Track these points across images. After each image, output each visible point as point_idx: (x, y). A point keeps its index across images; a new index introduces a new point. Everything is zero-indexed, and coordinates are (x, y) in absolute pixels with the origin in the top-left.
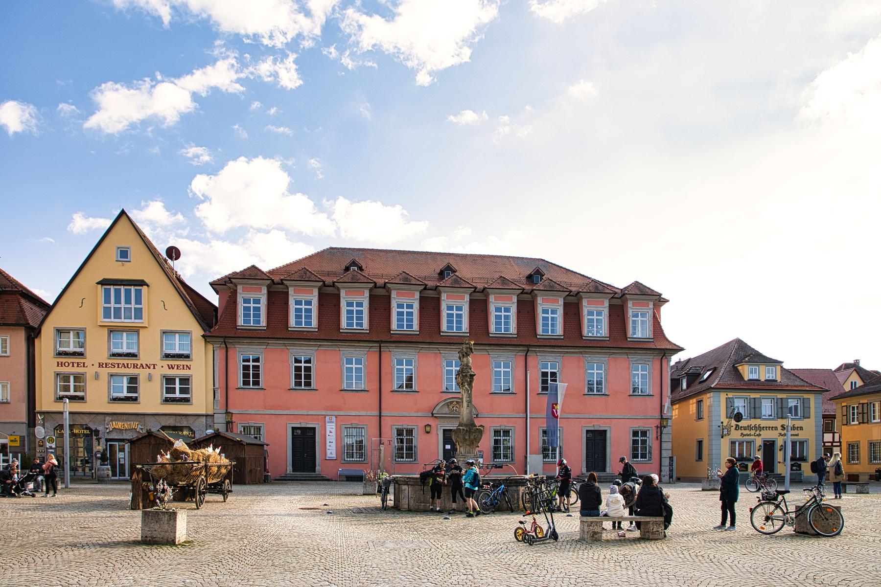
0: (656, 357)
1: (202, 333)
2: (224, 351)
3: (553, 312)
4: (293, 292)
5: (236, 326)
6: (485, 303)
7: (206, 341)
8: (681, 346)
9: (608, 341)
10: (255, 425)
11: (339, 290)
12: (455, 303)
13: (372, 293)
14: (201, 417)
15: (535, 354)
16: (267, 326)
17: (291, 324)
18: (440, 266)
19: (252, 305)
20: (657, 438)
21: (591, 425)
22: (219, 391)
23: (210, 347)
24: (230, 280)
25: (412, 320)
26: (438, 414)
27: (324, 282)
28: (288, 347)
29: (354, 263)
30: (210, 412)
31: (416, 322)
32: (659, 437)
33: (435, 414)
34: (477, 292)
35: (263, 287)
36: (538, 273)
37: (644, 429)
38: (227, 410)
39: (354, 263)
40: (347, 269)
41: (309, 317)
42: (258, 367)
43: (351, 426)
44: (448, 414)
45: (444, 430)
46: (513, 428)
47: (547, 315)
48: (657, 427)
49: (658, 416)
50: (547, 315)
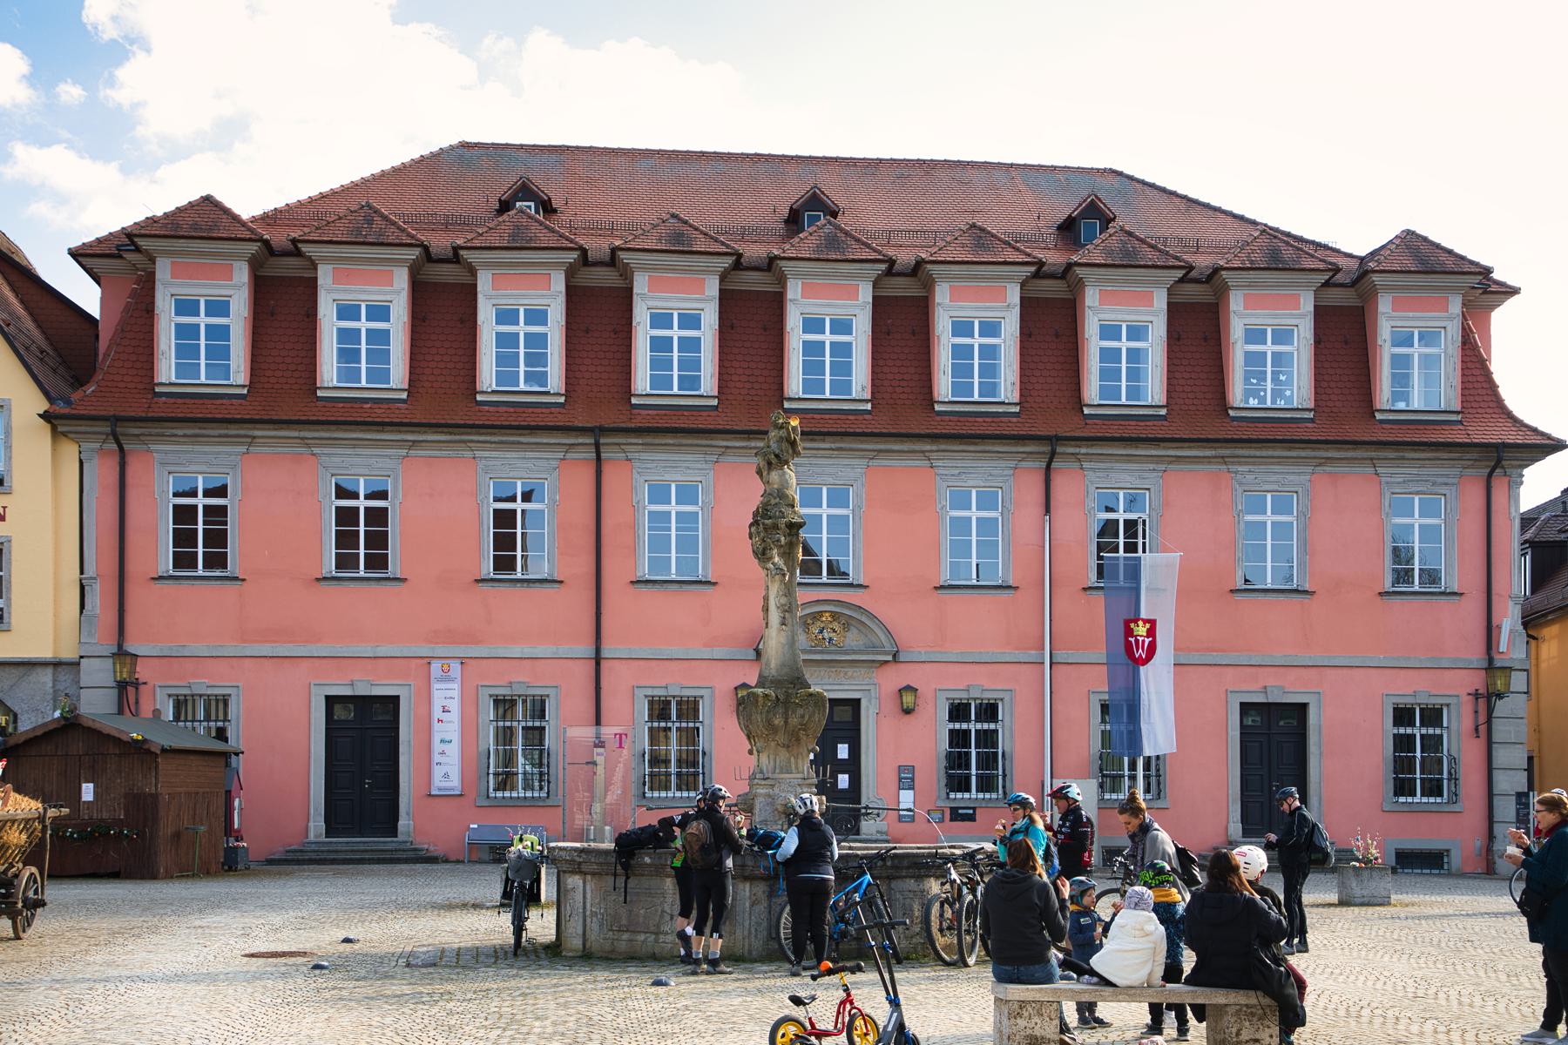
1: (43, 405)
2: (112, 465)
4: (330, 281)
7: (55, 433)
8: (1557, 434)
9: (1312, 421)
10: (209, 692)
11: (472, 272)
14: (39, 670)
16: (251, 386)
17: (326, 376)
18: (792, 193)
19: (203, 320)
20: (1477, 730)
22: (97, 587)
23: (70, 451)
24: (133, 243)
28: (316, 450)
29: (525, 191)
30: (68, 653)
32: (1483, 729)
35: (236, 265)
37: (1433, 701)
38: (120, 646)
39: (525, 191)
40: (505, 207)
41: (380, 356)
42: (223, 510)
47: (966, 340)
48: (1476, 695)
49: (1476, 656)
50: (966, 340)
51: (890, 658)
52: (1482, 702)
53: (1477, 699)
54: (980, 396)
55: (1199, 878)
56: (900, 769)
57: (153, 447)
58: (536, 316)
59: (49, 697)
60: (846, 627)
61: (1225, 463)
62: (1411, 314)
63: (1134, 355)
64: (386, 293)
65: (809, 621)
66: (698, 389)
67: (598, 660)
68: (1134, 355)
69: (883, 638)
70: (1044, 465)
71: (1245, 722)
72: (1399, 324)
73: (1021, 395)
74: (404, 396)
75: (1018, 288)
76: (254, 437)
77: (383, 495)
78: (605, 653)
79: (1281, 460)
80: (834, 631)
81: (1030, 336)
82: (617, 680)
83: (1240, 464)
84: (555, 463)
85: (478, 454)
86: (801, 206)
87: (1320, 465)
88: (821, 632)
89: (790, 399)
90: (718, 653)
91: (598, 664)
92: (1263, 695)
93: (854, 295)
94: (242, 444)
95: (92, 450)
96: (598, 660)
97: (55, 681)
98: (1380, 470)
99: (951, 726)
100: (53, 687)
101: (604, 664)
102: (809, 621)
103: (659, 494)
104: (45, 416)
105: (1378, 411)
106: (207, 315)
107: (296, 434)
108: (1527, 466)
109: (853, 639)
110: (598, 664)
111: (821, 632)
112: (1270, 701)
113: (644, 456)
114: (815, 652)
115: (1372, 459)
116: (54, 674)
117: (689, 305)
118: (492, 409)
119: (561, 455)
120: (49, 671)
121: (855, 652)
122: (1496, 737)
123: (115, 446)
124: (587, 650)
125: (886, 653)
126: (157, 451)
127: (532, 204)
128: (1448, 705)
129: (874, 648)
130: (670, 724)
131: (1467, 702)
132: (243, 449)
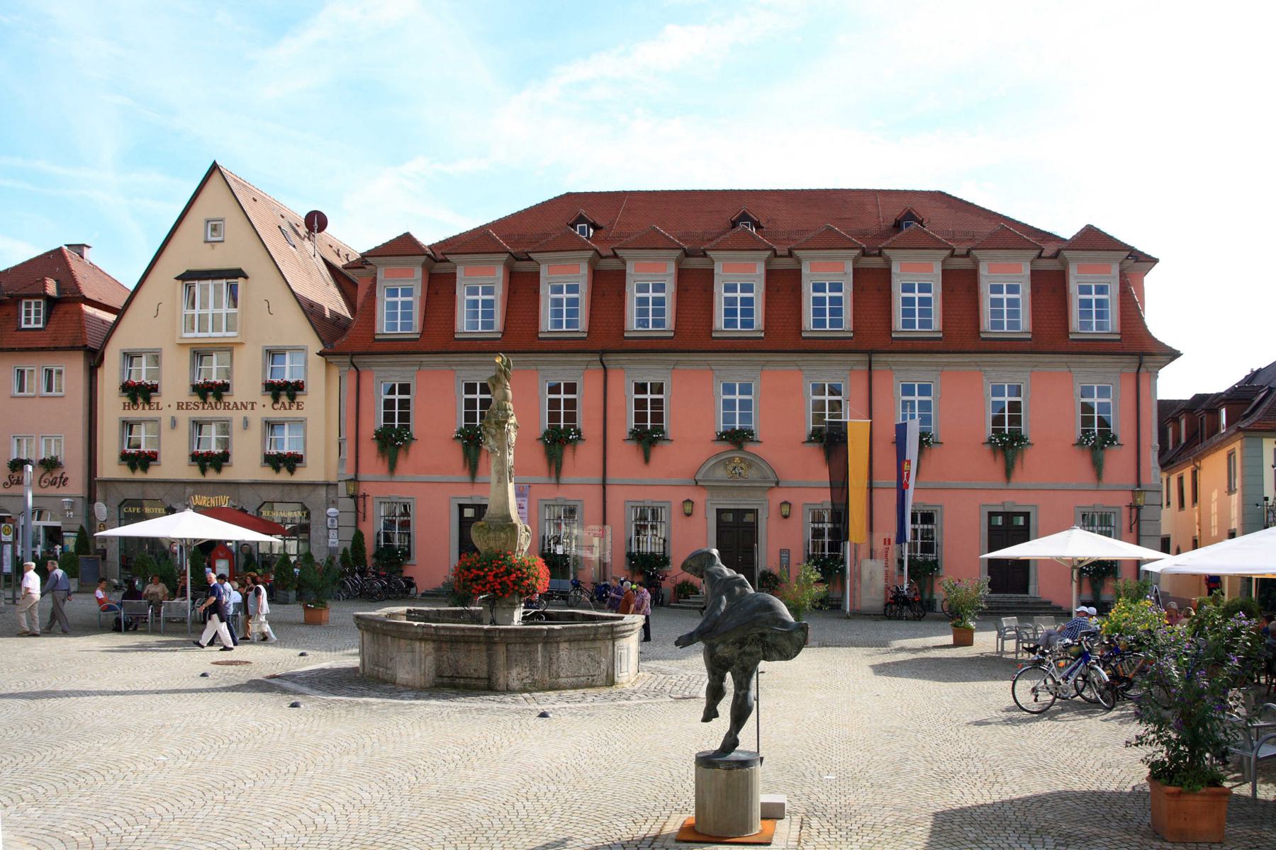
0: (1125, 370)
1: (319, 347)
2: (354, 377)
4: (463, 275)
5: (374, 334)
6: (1060, 279)
7: (328, 364)
8: (1175, 347)
9: (672, 338)
10: (401, 501)
11: (799, 262)
12: (740, 279)
13: (859, 266)
14: (320, 487)
15: (1066, 370)
16: (422, 334)
17: (898, 326)
18: (897, 212)
19: (828, 294)
20: (1131, 528)
21: (999, 502)
22: (346, 443)
23: (335, 372)
25: (662, 312)
26: (705, 481)
27: (775, 251)
28: (454, 368)
29: (744, 217)
30: (333, 479)
31: (670, 315)
32: (1134, 527)
33: (701, 481)
34: (1045, 258)
35: (416, 269)
36: (909, 216)
37: (1104, 510)
38: (356, 476)
39: (744, 217)
40: (734, 224)
41: (836, 312)
42: (661, 401)
43: (555, 503)
44: (727, 481)
45: (717, 510)
46: (938, 509)
48: (1131, 507)
49: (1130, 482)
51: (774, 485)
52: (1134, 511)
54: (1008, 329)
55: (478, 608)
56: (782, 551)
57: (373, 368)
58: (925, 288)
59: (324, 502)
60: (750, 466)
61: (978, 366)
62: (1089, 275)
63: (1012, 303)
66: (493, 329)
67: (604, 485)
70: (1135, 370)
71: (993, 523)
72: (1083, 281)
74: (500, 336)
75: (1029, 264)
77: (660, 391)
78: (608, 482)
79: (393, 364)
80: (742, 468)
81: (1038, 292)
82: (615, 495)
84: (848, 372)
85: (539, 367)
86: (737, 218)
87: (1036, 366)
88: (734, 469)
89: (717, 331)
90: (673, 480)
91: (604, 488)
94: (415, 365)
96: (604, 485)
98: (1072, 369)
101: (607, 487)
103: (729, 389)
104: (320, 354)
106: (741, 292)
109: (753, 474)
110: (604, 488)
111: (734, 469)
112: (1007, 510)
113: (631, 366)
114: (732, 481)
115: (1066, 363)
116: (327, 490)
117: (836, 280)
119: (849, 368)
120: (324, 488)
122: (1142, 533)
123: (354, 369)
124: (598, 479)
125: (771, 482)
128: (1114, 513)
129: (765, 479)
130: (646, 523)
131: (1125, 511)
132: (417, 368)
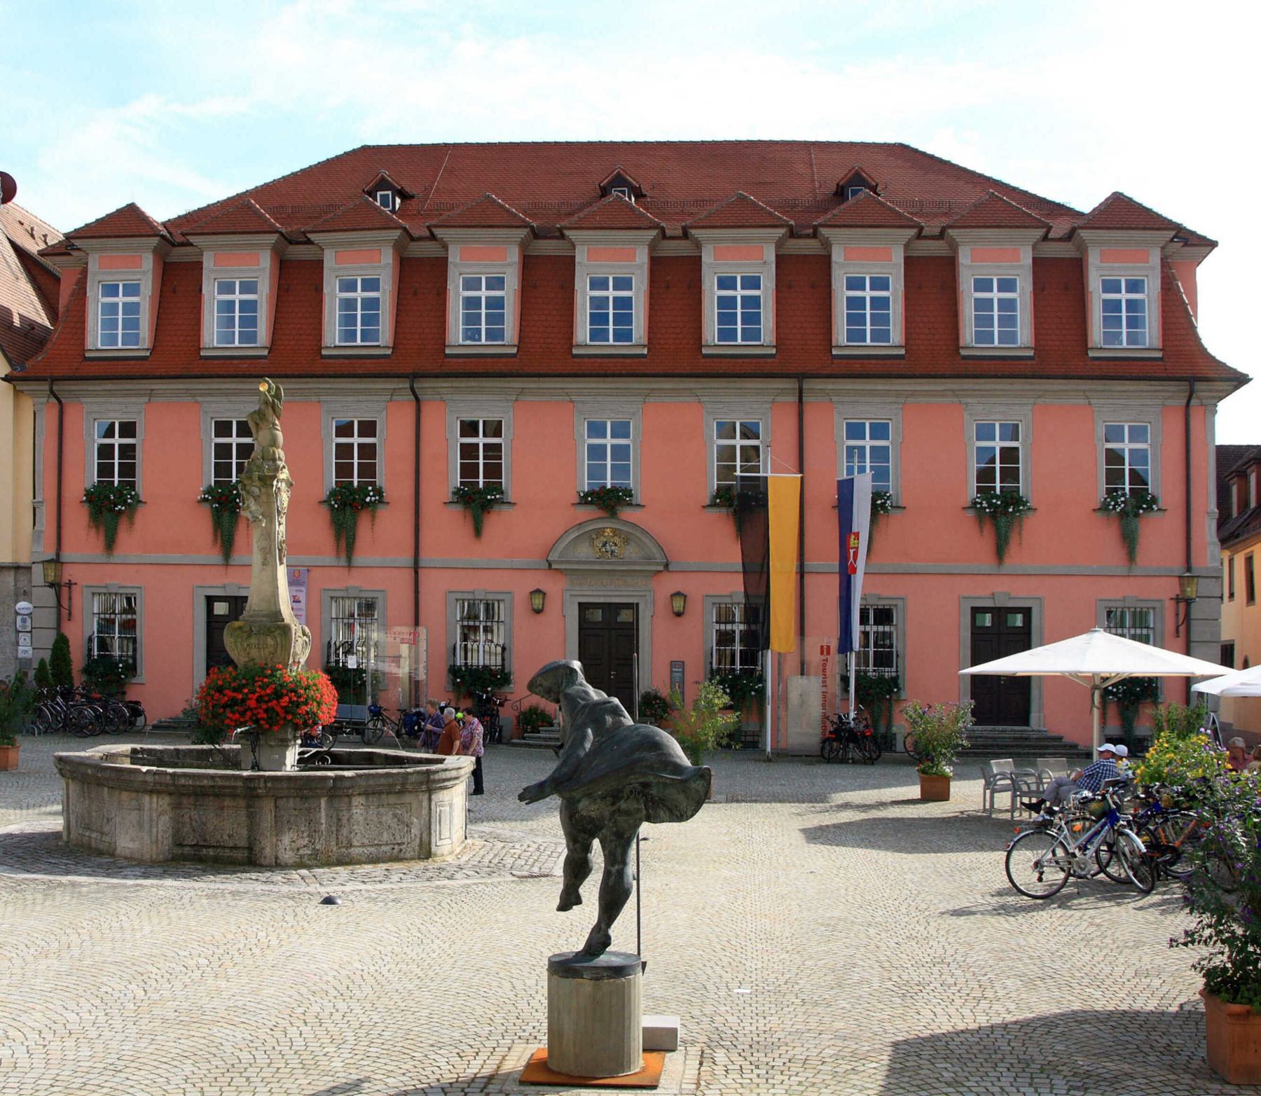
0: (1169, 402)
2: (55, 412)
3: (1134, 286)
5: (84, 350)
6: (1076, 270)
7: (17, 393)
8: (1242, 369)
10: (121, 591)
11: (698, 246)
12: (613, 271)
13: (783, 252)
15: (1082, 402)
16: (153, 350)
18: (838, 174)
20: (1177, 631)
21: (987, 593)
23: (28, 405)
24: (432, 234)
25: (500, 319)
26: (562, 562)
27: (663, 230)
28: (199, 399)
29: (619, 181)
30: (24, 560)
31: (511, 325)
32: (1182, 629)
33: (555, 562)
34: (1053, 240)
36: (857, 180)
37: (1140, 604)
38: (58, 555)
39: (619, 181)
41: (752, 318)
42: (498, 447)
43: (344, 594)
44: (594, 563)
45: (580, 604)
46: (900, 603)
48: (1177, 600)
49: (1177, 566)
51: (661, 568)
52: (1182, 606)
53: (1178, 603)
54: (999, 343)
55: (235, 747)
56: (673, 664)
57: (83, 400)
58: (881, 284)
59: (12, 593)
60: (627, 541)
61: (957, 396)
62: (1117, 265)
63: (1007, 305)
64: (255, 271)
65: (594, 536)
66: (255, 342)
67: (416, 568)
68: (131, 309)
69: (654, 550)
70: (1184, 402)
71: (978, 623)
72: (1107, 273)
73: (520, 337)
74: (266, 353)
75: (1029, 249)
76: (152, 390)
77: (497, 433)
78: (422, 564)
79: (111, 394)
80: (616, 545)
81: (1043, 289)
83: (969, 396)
84: (768, 406)
85: (322, 398)
86: (609, 183)
87: (1039, 397)
88: (604, 545)
90: (518, 562)
91: (416, 573)
92: (991, 601)
93: (632, 257)
94: (142, 395)
95: (42, 404)
96: (416, 568)
97: (16, 581)
98: (1093, 401)
99: (134, 617)
100: (15, 585)
101: (420, 571)
102: (594, 536)
103: (597, 429)
104: (7, 379)
105: (1092, 349)
107: (182, 386)
108: (1221, 399)
109: (631, 552)
110: (416, 573)
111: (604, 545)
112: (998, 605)
113: (456, 397)
114: (601, 563)
115: (1084, 391)
116: (15, 575)
117: (751, 272)
118: (346, 361)
120: (12, 573)
121: (634, 563)
122: (1194, 637)
123: (54, 400)
124: (407, 559)
125: (658, 564)
126: (86, 403)
127: (390, 193)
128: (1154, 608)
129: (649, 559)
130: (477, 623)
131: (1169, 606)
132: (146, 399)
